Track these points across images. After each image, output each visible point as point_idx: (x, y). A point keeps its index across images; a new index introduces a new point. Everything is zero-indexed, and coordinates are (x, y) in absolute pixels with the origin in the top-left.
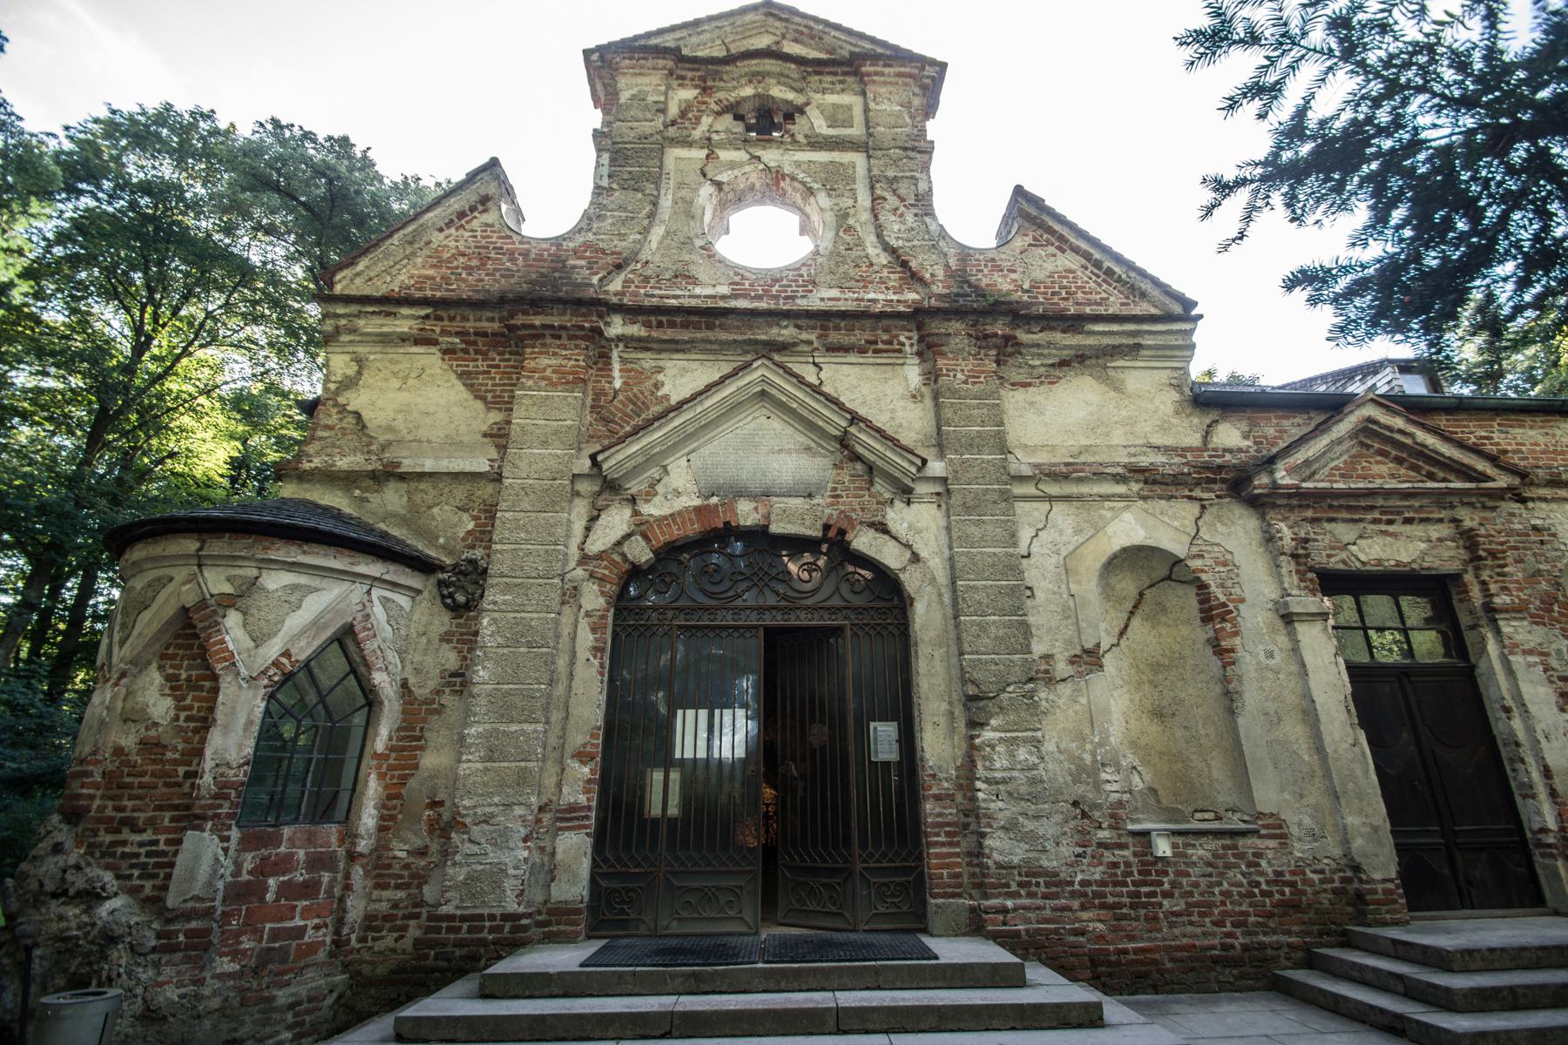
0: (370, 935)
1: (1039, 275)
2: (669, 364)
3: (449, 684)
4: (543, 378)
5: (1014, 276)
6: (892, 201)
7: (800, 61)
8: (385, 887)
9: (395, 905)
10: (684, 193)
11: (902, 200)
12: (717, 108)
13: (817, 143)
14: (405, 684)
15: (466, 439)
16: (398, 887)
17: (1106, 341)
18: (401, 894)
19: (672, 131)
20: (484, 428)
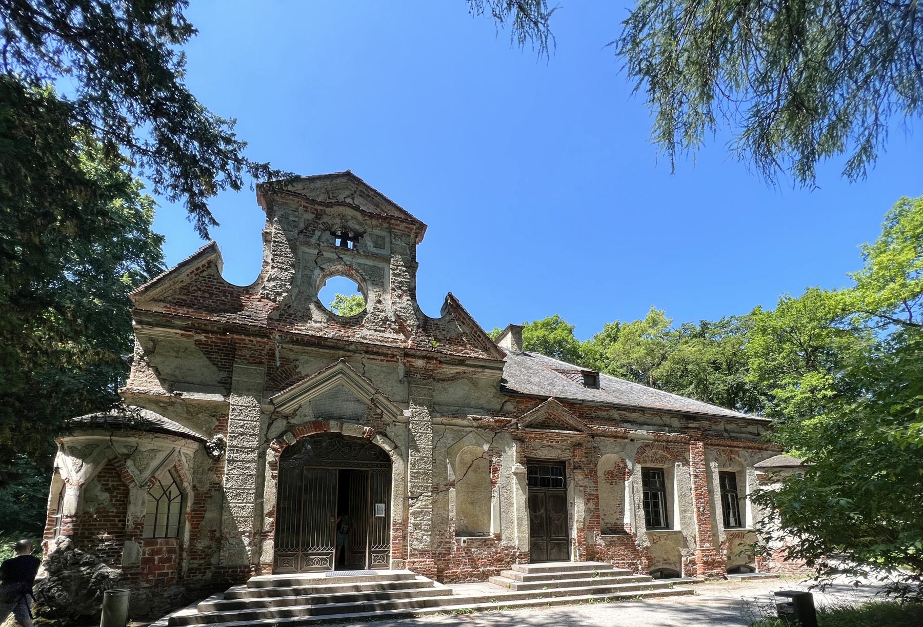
0: (191, 575)
2: (301, 358)
3: (213, 487)
4: (246, 359)
7: (363, 212)
8: (196, 559)
9: (200, 565)
10: (307, 272)
12: (323, 227)
13: (368, 255)
14: (194, 487)
15: (211, 383)
16: (200, 559)
18: (202, 561)
20: (219, 379)
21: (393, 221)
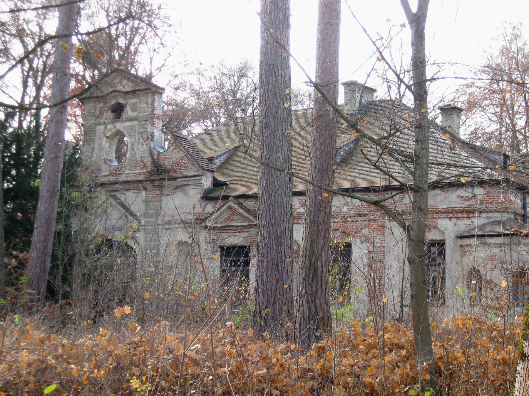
1: (174, 159)
5: (169, 160)
6: (141, 139)
11: (144, 139)
17: (182, 183)
19: (97, 122)
21: (137, 93)
